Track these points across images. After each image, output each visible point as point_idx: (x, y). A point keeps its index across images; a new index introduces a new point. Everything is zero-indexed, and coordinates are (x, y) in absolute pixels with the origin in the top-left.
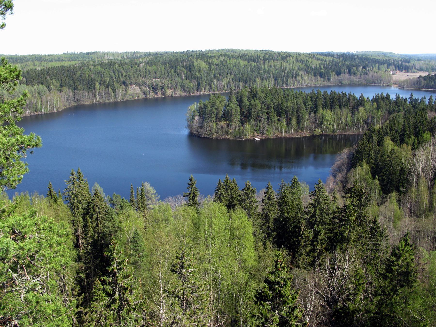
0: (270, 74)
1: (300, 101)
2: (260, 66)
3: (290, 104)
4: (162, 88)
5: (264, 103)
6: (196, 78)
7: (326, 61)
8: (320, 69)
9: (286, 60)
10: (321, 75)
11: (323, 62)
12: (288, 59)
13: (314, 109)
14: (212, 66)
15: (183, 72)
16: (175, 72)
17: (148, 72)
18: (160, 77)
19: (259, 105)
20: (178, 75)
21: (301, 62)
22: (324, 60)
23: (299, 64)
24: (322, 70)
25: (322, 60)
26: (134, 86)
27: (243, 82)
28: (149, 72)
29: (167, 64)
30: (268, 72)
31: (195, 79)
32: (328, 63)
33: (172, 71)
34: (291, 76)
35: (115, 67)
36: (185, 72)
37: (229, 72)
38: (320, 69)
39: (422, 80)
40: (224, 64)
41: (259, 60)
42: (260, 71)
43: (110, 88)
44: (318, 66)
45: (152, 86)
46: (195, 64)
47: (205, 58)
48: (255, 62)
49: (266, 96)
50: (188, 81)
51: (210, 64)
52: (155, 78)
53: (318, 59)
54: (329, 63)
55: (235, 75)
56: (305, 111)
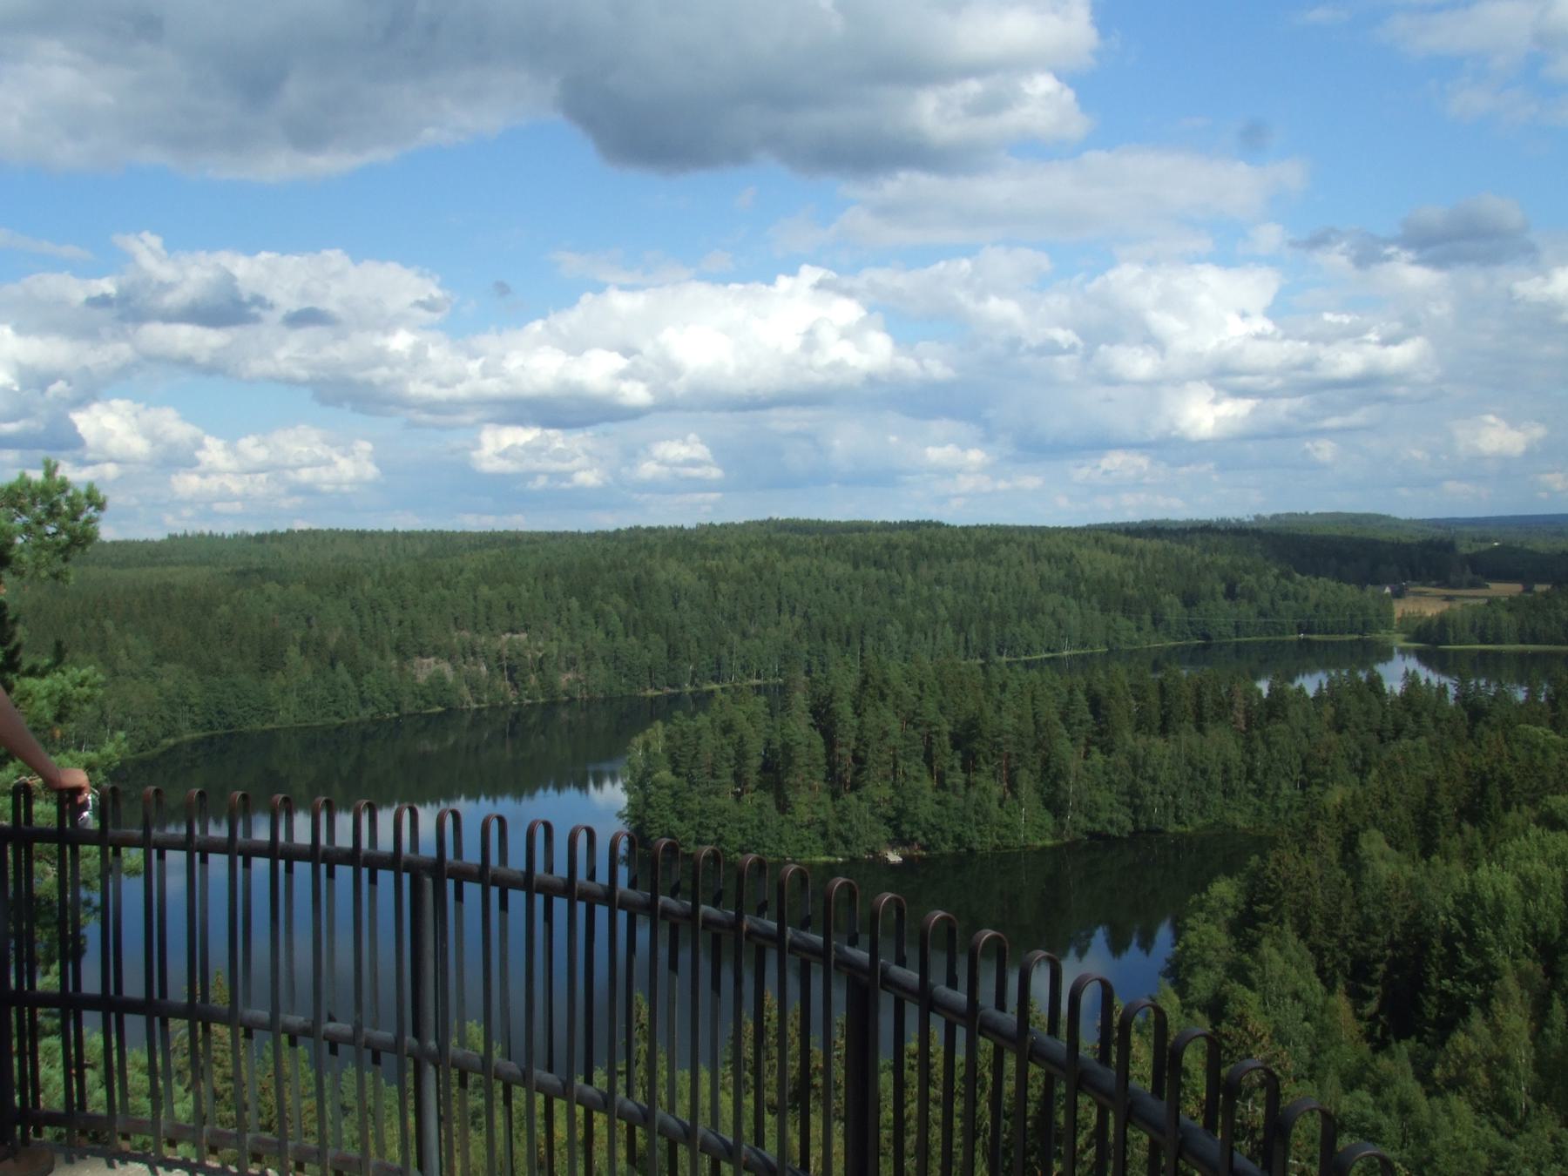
1: (1050, 711)
2: (898, 580)
3: (1009, 721)
5: (912, 720)
7: (1142, 554)
8: (1122, 586)
9: (993, 558)
10: (1128, 608)
11: (1133, 561)
12: (1002, 549)
13: (1102, 738)
14: (722, 585)
15: (616, 607)
16: (583, 608)
17: (482, 609)
18: (527, 628)
19: (895, 725)
20: (596, 617)
21: (1049, 561)
23: (1044, 567)
24: (1129, 592)
25: (1126, 552)
26: (432, 660)
28: (489, 606)
29: (556, 580)
32: (1149, 565)
33: (575, 603)
34: (1014, 614)
35: (362, 590)
36: (623, 605)
37: (785, 606)
39: (1504, 615)
40: (767, 575)
42: (901, 602)
43: (340, 666)
44: (1115, 575)
45: (499, 659)
46: (661, 576)
47: (696, 555)
48: (877, 564)
49: (919, 693)
50: (633, 640)
52: (513, 631)
53: (1114, 549)
55: (806, 616)
56: (1068, 744)
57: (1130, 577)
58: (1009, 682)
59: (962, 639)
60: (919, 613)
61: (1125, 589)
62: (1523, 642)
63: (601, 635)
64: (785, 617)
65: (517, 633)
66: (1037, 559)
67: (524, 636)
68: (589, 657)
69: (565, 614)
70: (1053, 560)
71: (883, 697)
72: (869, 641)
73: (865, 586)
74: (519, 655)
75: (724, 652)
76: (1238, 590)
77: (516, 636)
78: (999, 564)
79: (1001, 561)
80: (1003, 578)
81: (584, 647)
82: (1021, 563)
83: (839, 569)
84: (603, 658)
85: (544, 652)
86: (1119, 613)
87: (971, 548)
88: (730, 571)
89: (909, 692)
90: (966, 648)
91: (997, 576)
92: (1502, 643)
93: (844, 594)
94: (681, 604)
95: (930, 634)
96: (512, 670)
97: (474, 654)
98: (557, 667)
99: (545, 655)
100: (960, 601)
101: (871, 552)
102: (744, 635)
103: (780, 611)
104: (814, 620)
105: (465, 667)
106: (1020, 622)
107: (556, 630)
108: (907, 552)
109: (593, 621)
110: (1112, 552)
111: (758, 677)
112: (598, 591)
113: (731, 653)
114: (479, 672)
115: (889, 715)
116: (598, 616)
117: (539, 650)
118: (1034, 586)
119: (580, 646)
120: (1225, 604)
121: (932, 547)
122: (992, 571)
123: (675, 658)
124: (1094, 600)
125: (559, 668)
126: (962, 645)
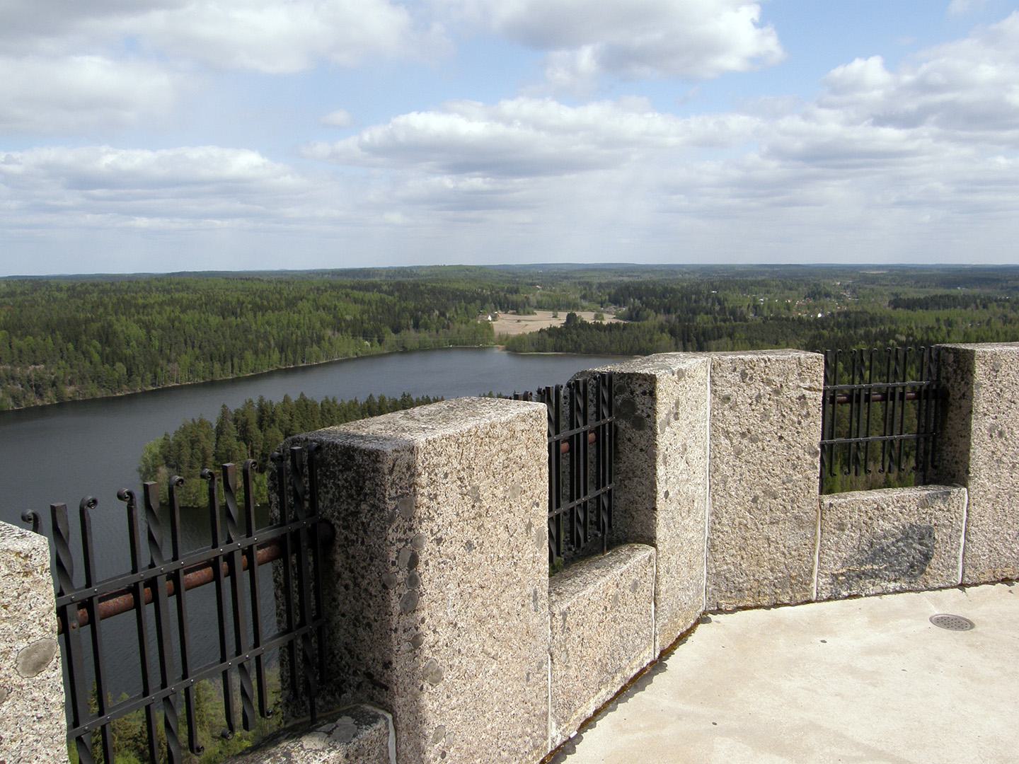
0: (269, 342)
4: (54, 384)
6: (123, 359)
7: (370, 303)
8: (362, 323)
10: (366, 335)
11: (366, 307)
14: (153, 331)
15: (95, 347)
16: (76, 348)
17: (16, 351)
18: (44, 362)
19: (281, 437)
20: (83, 353)
21: (324, 309)
22: (367, 301)
23: (322, 313)
24: (366, 325)
25: (362, 302)
27: (219, 361)
29: (58, 332)
30: (266, 338)
31: (120, 360)
33: (71, 346)
34: (309, 341)
36: (99, 345)
38: (362, 323)
39: (546, 336)
40: (177, 324)
41: (244, 310)
42: (250, 337)
45: (29, 381)
46: (117, 327)
47: (133, 310)
50: (107, 366)
51: (148, 327)
52: (35, 364)
53: (356, 301)
54: (376, 309)
57: (365, 317)
58: (331, 408)
59: (283, 356)
60: (260, 344)
61: (364, 325)
62: (556, 351)
63: (88, 364)
64: (190, 349)
65: (38, 365)
66: (318, 309)
67: (42, 366)
68: (83, 378)
69: (65, 352)
70: (326, 309)
71: (273, 421)
72: (236, 360)
73: (230, 327)
74: (41, 379)
75: (159, 370)
76: (420, 323)
77: (37, 367)
78: (299, 312)
79: (300, 311)
80: (302, 321)
81: (80, 372)
82: (311, 312)
83: (215, 320)
84: (91, 377)
85: (55, 375)
86: (361, 338)
87: (283, 303)
88: (157, 323)
89: (287, 417)
90: (286, 360)
91: (299, 320)
92: (546, 352)
93: (220, 334)
94: (131, 344)
95: (267, 354)
96: (37, 387)
97: (13, 378)
98: (63, 382)
99: (56, 377)
100: (281, 335)
101: (230, 306)
102: (169, 361)
103: (186, 344)
104: (205, 350)
105: (9, 386)
106: (312, 344)
107: (62, 363)
108: (250, 306)
109: (82, 356)
110: (355, 303)
111: (177, 382)
112: (84, 338)
113: (162, 370)
114: (18, 390)
115: (278, 431)
116: (86, 354)
117: (52, 374)
118: (318, 325)
119: (77, 371)
120: (412, 332)
121: (262, 303)
122: (296, 317)
123: (131, 375)
124: (349, 330)
125: (63, 382)
126: (283, 359)
